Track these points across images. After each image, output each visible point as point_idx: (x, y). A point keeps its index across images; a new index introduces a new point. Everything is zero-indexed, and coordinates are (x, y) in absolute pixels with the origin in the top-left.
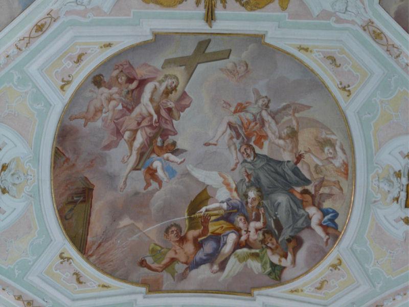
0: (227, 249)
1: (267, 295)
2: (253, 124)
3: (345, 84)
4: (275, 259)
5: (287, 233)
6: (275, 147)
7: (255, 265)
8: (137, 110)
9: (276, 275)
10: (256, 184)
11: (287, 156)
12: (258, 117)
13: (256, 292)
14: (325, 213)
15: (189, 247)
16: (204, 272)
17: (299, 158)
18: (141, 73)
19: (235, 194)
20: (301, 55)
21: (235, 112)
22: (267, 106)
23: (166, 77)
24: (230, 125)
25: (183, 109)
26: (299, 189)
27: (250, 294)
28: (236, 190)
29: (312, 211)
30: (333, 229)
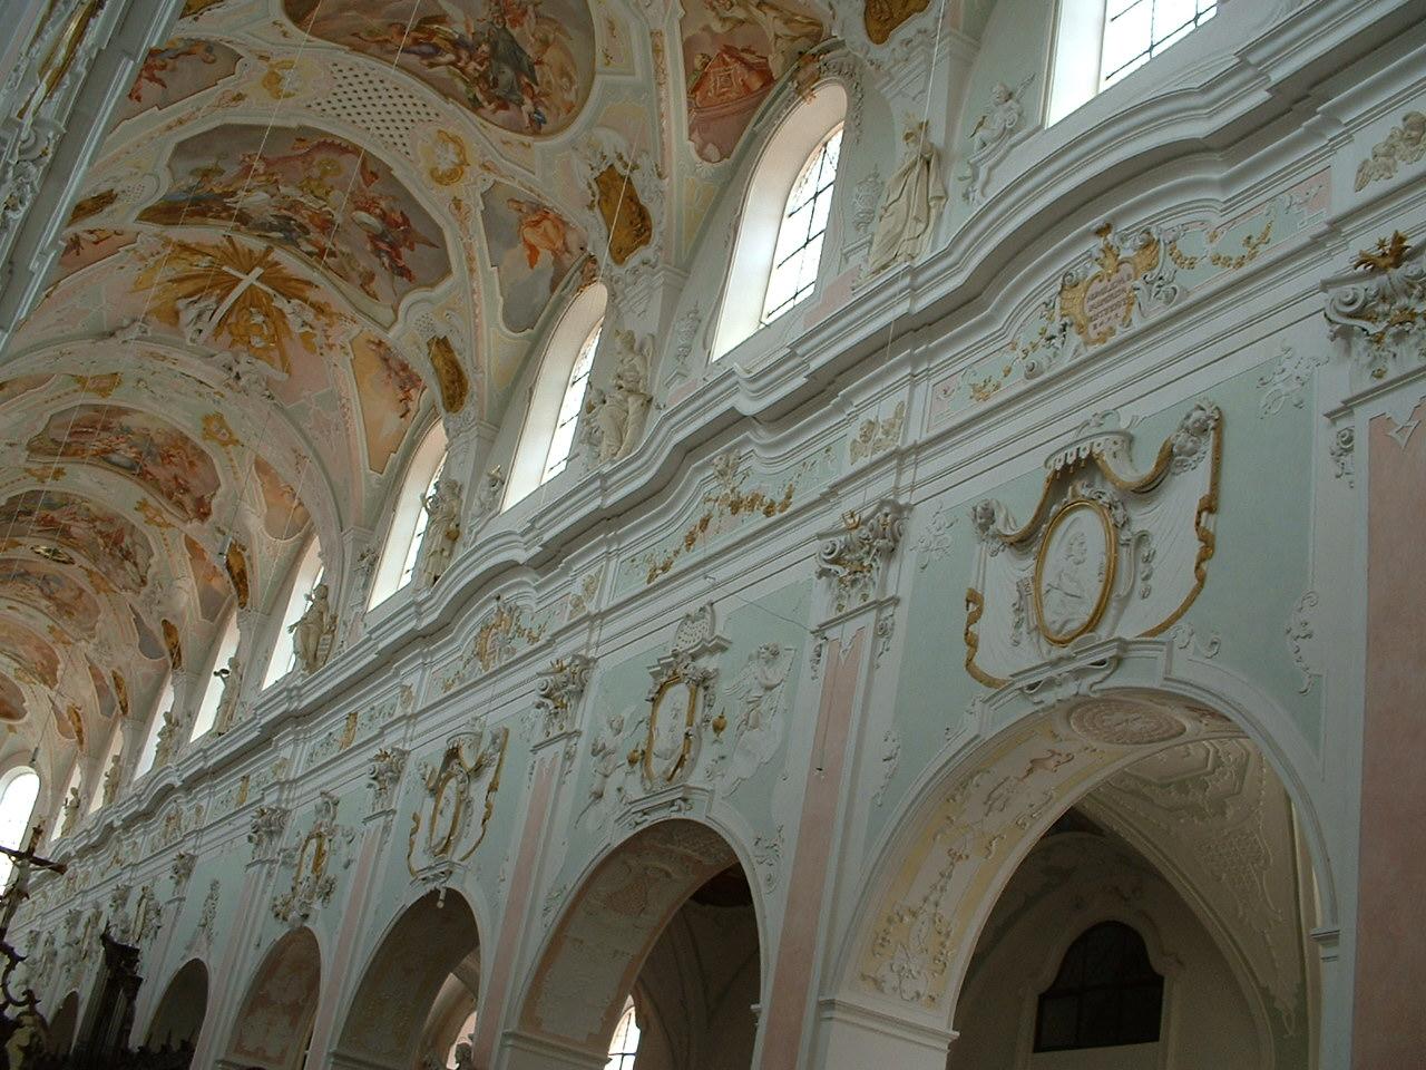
0: (442, 59)
1: (462, 111)
3: (611, 54)
4: (480, 97)
5: (502, 94)
6: (525, 34)
7: (462, 87)
9: (475, 105)
10: (494, 47)
11: (529, 52)
12: (524, 6)
14: (536, 112)
16: (413, 60)
17: (540, 62)
19: (470, 36)
22: (536, 5)
26: (526, 80)
29: (528, 101)
30: (536, 127)
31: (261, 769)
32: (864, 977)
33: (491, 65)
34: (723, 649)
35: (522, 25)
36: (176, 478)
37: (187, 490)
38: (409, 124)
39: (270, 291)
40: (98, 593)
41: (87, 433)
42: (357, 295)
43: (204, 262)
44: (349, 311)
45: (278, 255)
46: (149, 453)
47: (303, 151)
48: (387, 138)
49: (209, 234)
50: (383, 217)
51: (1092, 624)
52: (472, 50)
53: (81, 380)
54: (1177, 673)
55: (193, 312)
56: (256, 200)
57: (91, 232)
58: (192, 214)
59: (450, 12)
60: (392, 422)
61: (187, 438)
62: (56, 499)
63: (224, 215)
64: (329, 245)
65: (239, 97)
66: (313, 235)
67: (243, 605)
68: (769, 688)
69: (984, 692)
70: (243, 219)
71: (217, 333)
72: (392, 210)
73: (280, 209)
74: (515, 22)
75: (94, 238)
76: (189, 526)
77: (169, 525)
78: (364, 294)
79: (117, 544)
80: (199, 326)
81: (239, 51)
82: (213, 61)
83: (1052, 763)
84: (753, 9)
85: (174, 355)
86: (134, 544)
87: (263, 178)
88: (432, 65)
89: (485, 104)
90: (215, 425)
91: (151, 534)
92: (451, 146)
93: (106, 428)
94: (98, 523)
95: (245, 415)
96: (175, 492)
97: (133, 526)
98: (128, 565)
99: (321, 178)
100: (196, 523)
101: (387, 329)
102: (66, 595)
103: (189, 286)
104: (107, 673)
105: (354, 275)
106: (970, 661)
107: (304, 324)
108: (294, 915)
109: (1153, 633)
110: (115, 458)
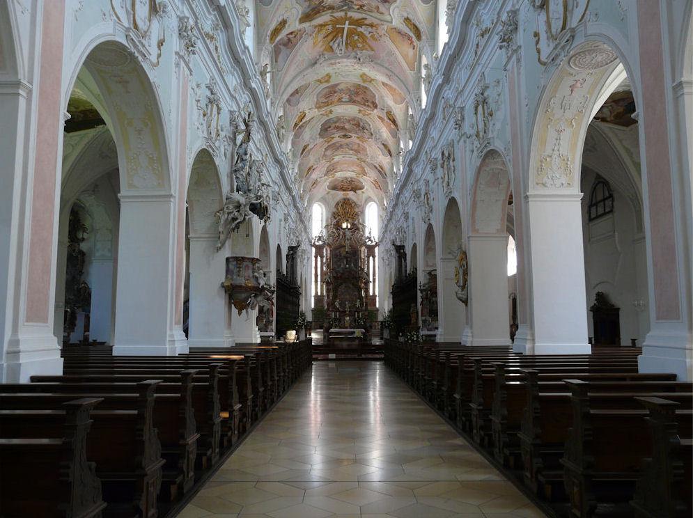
31: (412, 180)
32: (537, 184)
34: (488, 87)
39: (354, 27)
41: (331, 94)
43: (330, 27)
44: (379, 22)
45: (350, 14)
51: (564, 27)
53: (319, 81)
54: (589, 32)
55: (336, 45)
57: (291, 33)
60: (411, 52)
62: (335, 120)
68: (499, 95)
69: (543, 68)
70: (331, 8)
71: (347, 48)
75: (293, 36)
77: (370, 114)
79: (359, 126)
83: (579, 85)
90: (363, 76)
91: (367, 119)
93: (335, 92)
95: (366, 70)
97: (361, 119)
98: (365, 131)
101: (392, 22)
102: (355, 147)
104: (377, 166)
106: (539, 59)
108: (427, 219)
109: (580, 21)
110: (343, 100)
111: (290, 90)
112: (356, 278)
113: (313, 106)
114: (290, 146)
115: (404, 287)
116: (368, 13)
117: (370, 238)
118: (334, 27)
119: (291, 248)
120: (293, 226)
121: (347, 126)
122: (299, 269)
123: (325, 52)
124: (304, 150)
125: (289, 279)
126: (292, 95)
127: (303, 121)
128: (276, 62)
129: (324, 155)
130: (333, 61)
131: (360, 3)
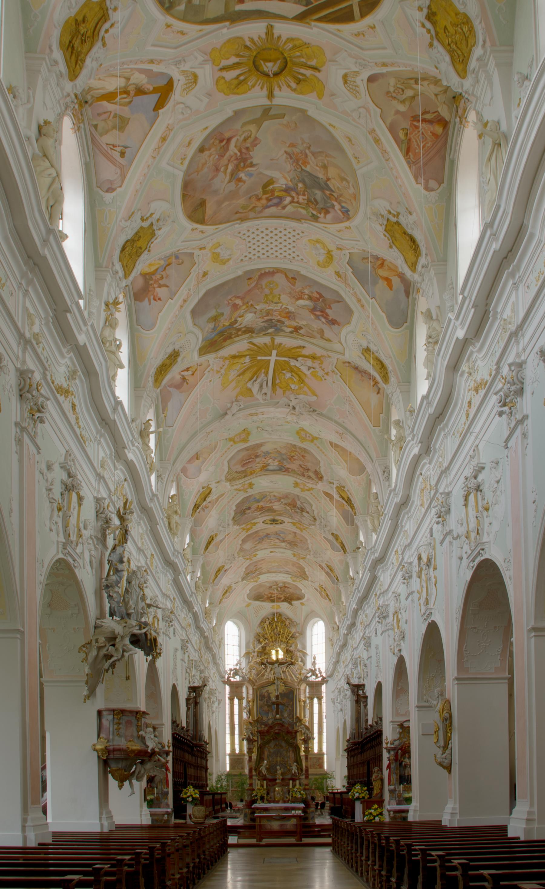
2: (300, 155)
4: (315, 213)
7: (304, 212)
8: (227, 155)
9: (315, 218)
10: (303, 182)
13: (303, 221)
15: (264, 202)
16: (273, 210)
18: (227, 135)
19: (290, 183)
20: (331, 129)
21: (289, 146)
22: (309, 148)
23: (244, 132)
24: (286, 152)
25: (256, 145)
27: (300, 220)
28: (291, 181)
33: (308, 193)
35: (308, 163)
36: (301, 466)
37: (308, 470)
38: (294, 244)
39: (287, 359)
40: (302, 531)
42: (322, 343)
43: (247, 359)
44: (324, 353)
45: (278, 340)
46: (284, 459)
47: (253, 285)
48: (288, 257)
49: (240, 345)
50: (310, 298)
52: (295, 189)
53: (231, 440)
56: (249, 319)
57: (187, 369)
58: (225, 340)
59: (273, 175)
61: (295, 445)
62: (258, 497)
63: (240, 333)
64: (296, 324)
65: (205, 274)
66: (287, 322)
67: (355, 514)
70: (249, 330)
72: (312, 293)
73: (263, 318)
74: (305, 163)
75: (190, 372)
76: (318, 486)
77: (312, 489)
78: (325, 341)
79: (296, 506)
80: (264, 391)
81: (189, 251)
82: (183, 263)
84: (415, 86)
85: (261, 410)
86: (302, 503)
87: (244, 307)
88: (284, 208)
89: (319, 215)
90: (301, 433)
91: (306, 495)
92: (318, 246)
93: (257, 456)
94: (282, 500)
95: (307, 423)
96: (304, 471)
98: (304, 514)
99: (271, 293)
100: (320, 483)
102: (290, 537)
103: (248, 375)
104: (323, 565)
105: (315, 334)
107: (309, 368)
110: (270, 468)
111: (186, 455)
112: (291, 733)
113: (223, 478)
114: (188, 540)
115: (363, 746)
116: (306, 338)
117: (313, 672)
118: (253, 359)
119: (193, 689)
120: (195, 656)
121: (276, 506)
122: (206, 717)
123: (240, 397)
124: (209, 543)
125: (191, 732)
126: (190, 461)
127: (208, 500)
128: (164, 410)
129: (242, 550)
130: (254, 412)
131: (294, 324)
